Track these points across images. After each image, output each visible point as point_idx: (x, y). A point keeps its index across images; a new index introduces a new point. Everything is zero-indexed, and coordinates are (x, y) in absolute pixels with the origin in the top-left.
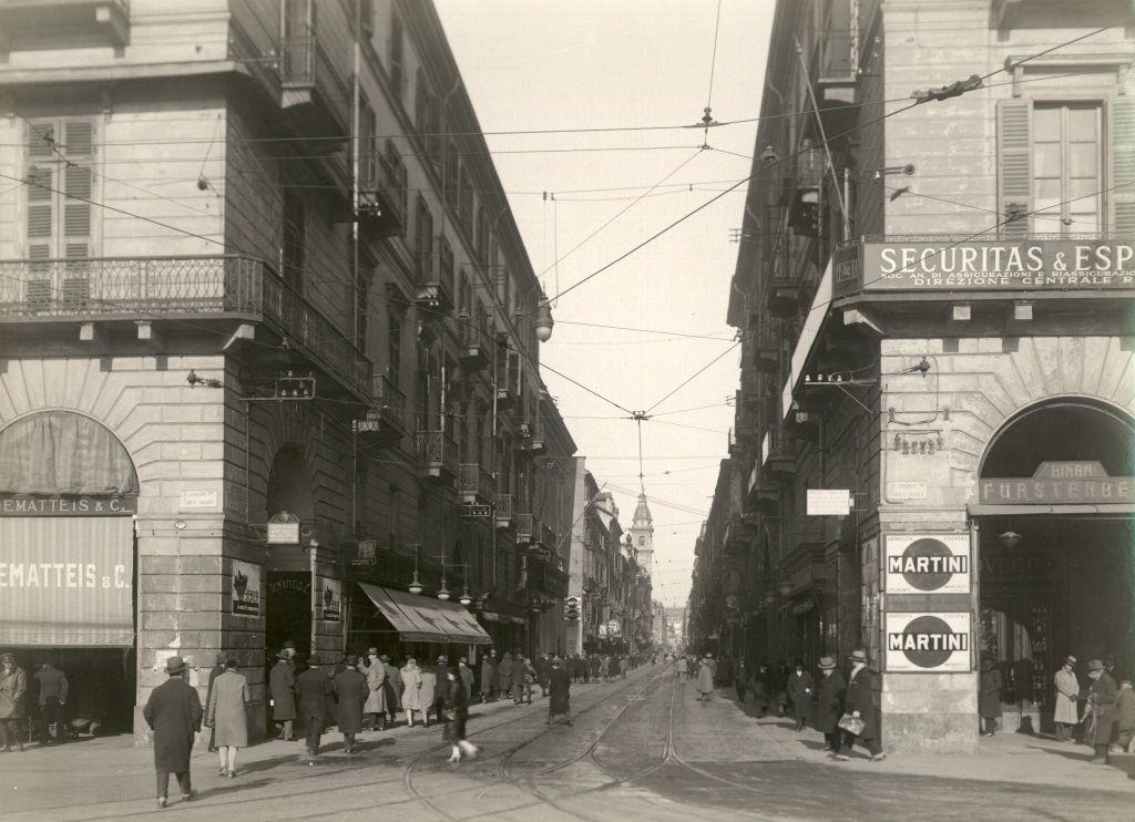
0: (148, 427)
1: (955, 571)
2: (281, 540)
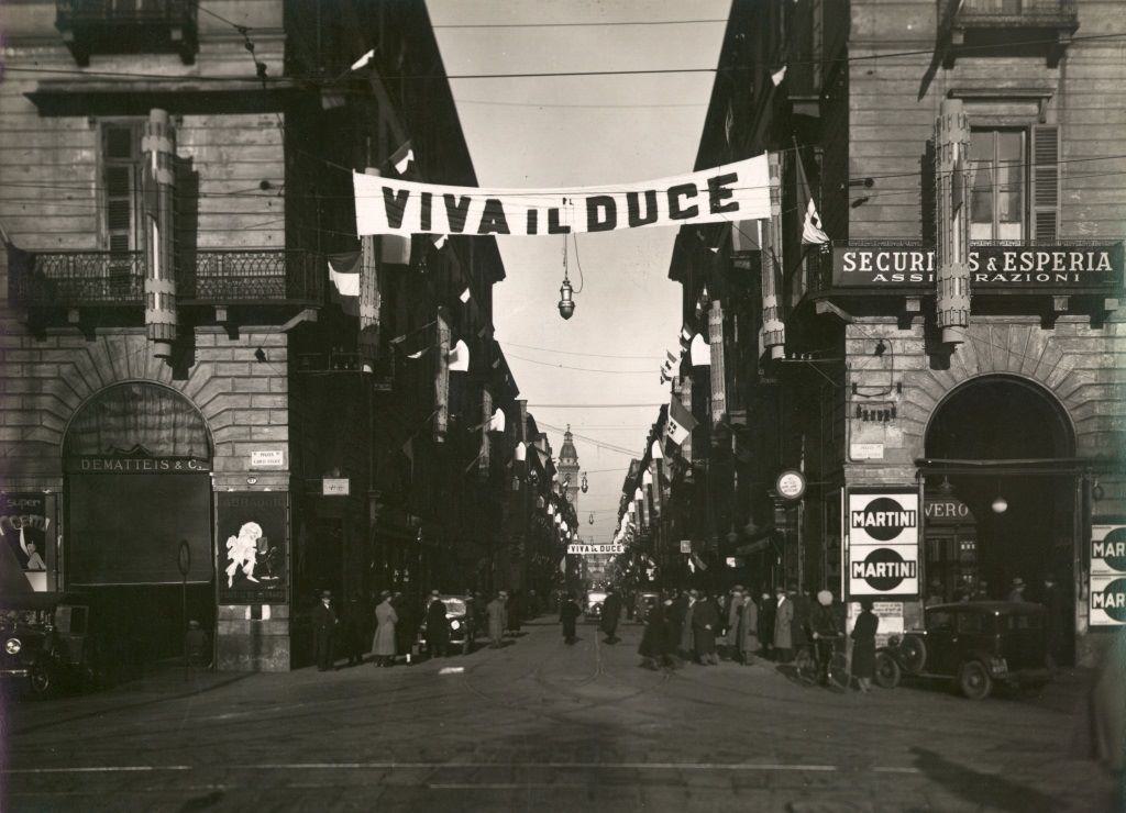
0: (221, 397)
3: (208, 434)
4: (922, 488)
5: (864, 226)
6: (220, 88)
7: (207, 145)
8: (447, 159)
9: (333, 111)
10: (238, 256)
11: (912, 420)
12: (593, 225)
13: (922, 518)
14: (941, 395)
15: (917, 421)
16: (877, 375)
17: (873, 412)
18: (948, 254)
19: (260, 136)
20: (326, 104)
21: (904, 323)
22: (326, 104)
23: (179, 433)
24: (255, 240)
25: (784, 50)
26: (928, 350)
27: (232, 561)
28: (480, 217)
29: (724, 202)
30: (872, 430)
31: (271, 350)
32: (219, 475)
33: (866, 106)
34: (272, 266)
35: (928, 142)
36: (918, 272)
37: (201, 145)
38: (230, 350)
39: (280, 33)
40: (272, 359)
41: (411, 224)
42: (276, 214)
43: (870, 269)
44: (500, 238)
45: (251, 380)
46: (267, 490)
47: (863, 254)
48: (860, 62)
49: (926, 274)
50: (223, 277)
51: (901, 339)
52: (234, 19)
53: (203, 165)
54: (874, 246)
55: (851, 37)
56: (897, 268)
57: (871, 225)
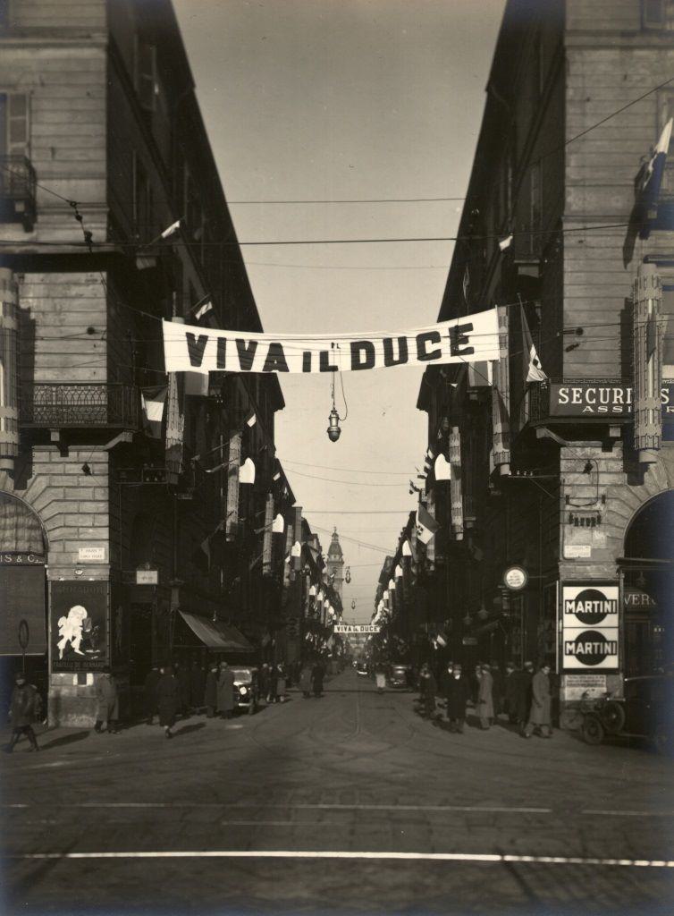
1: (608, 613)
3: (44, 533)
4: (622, 581)
10: (69, 388)
12: (356, 365)
13: (622, 606)
14: (637, 505)
15: (618, 527)
16: (586, 489)
17: (583, 519)
18: (643, 389)
19: (87, 291)
20: (140, 264)
21: (607, 447)
22: (140, 264)
23: (20, 533)
24: (83, 375)
25: (511, 222)
26: (626, 470)
27: (62, 637)
28: (265, 358)
29: (462, 347)
30: (582, 533)
31: (95, 465)
34: (96, 397)
35: (626, 299)
36: (619, 404)
37: (38, 298)
39: (104, 207)
41: (209, 364)
42: (100, 354)
43: (580, 402)
44: (281, 375)
45: (78, 490)
46: (91, 579)
47: (575, 390)
49: (625, 406)
50: (57, 406)
51: (605, 459)
54: (583, 383)
55: (566, 213)
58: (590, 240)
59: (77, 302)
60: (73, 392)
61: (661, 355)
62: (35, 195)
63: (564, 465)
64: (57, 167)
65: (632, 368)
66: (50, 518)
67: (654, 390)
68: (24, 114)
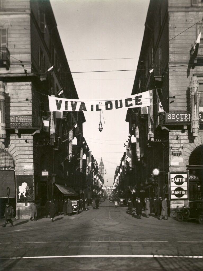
0: (17, 152)
1: (184, 182)
2: (45, 175)
3: (14, 161)
5: (173, 108)
6: (16, 76)
7: (13, 90)
8: (71, 93)
9: (43, 81)
10: (21, 117)
11: (186, 155)
12: (107, 109)
14: (192, 149)
15: (187, 156)
16: (177, 144)
17: (176, 154)
20: (41, 79)
21: (183, 132)
22: (41, 79)
23: (7, 161)
24: (25, 113)
25: (153, 64)
26: (189, 139)
27: (20, 192)
28: (80, 107)
29: (139, 102)
30: (176, 158)
31: (29, 140)
32: (17, 171)
33: (173, 78)
34: (29, 119)
35: (188, 87)
36: (186, 119)
37: (11, 90)
38: (19, 140)
40: (29, 142)
41: (63, 109)
43: (175, 118)
44: (84, 112)
45: (24, 148)
46: (28, 174)
47: (173, 115)
48: (172, 67)
49: (188, 119)
50: (17, 122)
51: (183, 136)
52: (19, 59)
53: (12, 95)
55: (169, 61)
56: (181, 118)
57: (175, 107)
58: (177, 70)
59: (23, 91)
60: (22, 118)
61: (199, 104)
62: (9, 59)
63: (170, 137)
64: (16, 51)
65: (190, 108)
66: (16, 156)
67: (197, 114)
68: (6, 35)
